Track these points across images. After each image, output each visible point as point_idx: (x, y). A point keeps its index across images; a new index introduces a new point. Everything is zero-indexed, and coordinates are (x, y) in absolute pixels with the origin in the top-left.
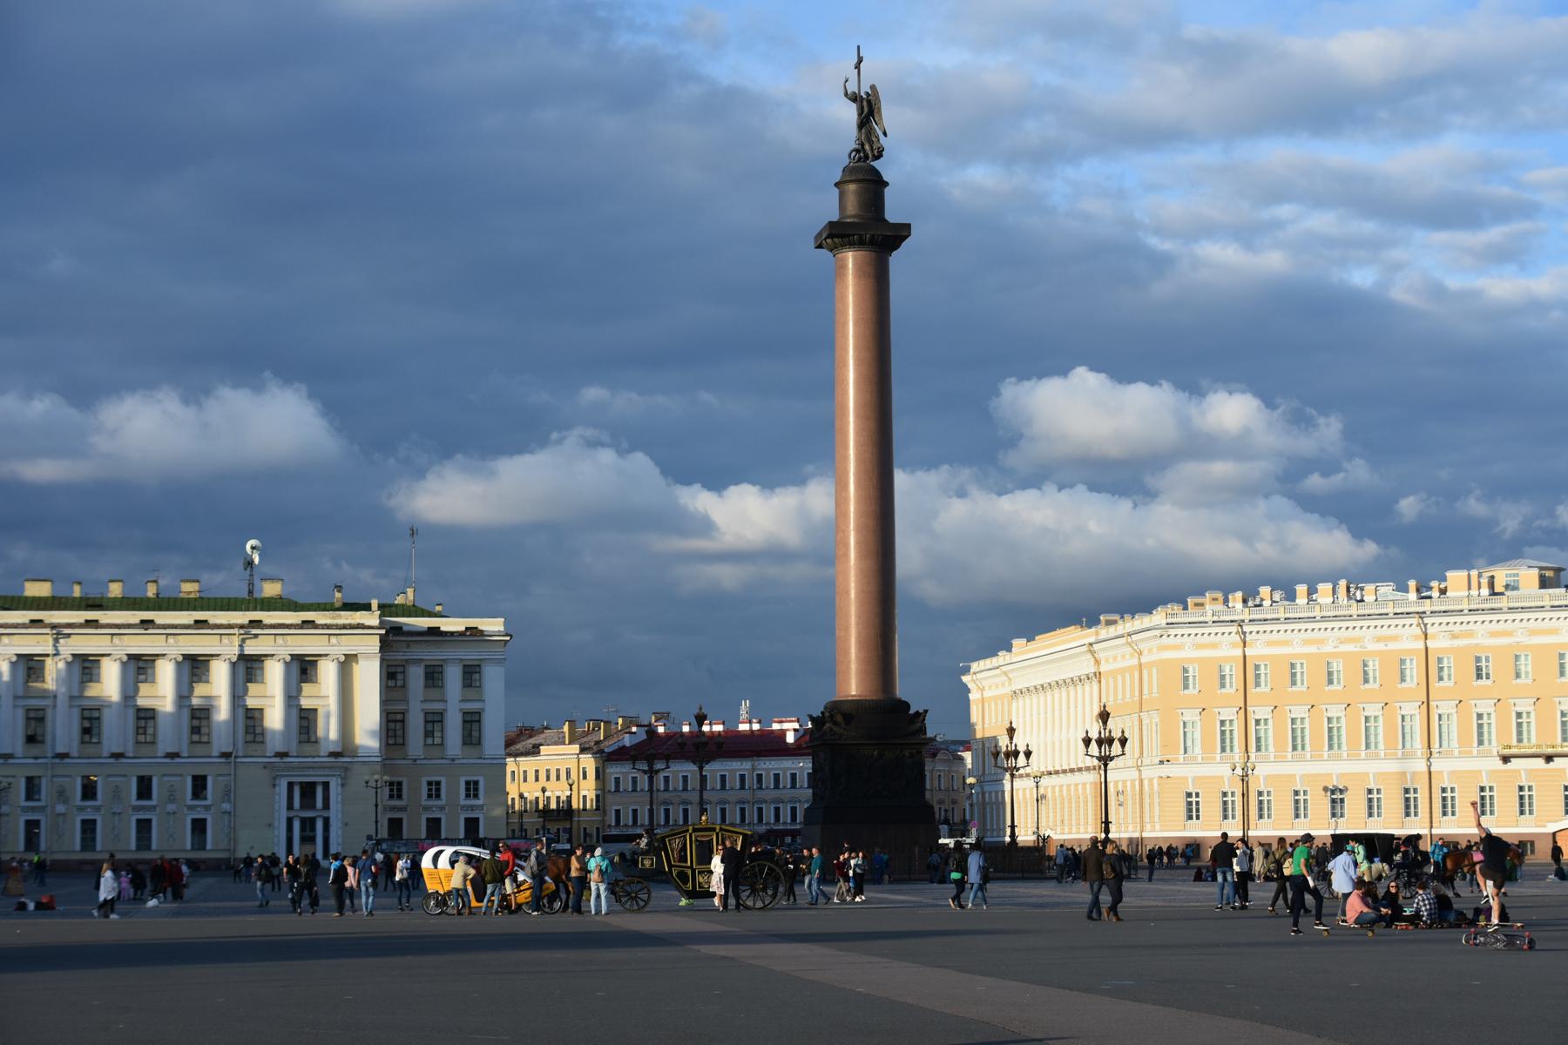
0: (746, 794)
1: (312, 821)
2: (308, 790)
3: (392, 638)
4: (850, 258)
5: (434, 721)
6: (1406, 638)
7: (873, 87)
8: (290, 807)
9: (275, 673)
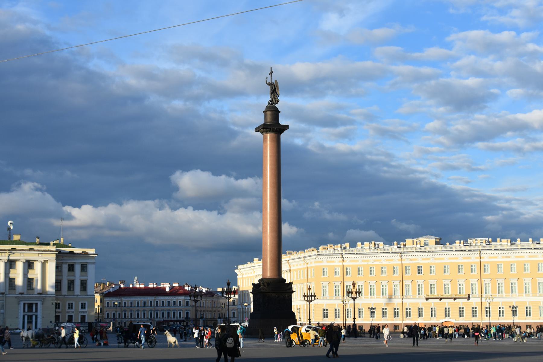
0: (152, 308)
1: (31, 316)
2: (30, 306)
3: (60, 255)
4: (268, 135)
5: (71, 283)
6: (395, 260)
7: (276, 81)
8: (24, 311)
9: (20, 266)
